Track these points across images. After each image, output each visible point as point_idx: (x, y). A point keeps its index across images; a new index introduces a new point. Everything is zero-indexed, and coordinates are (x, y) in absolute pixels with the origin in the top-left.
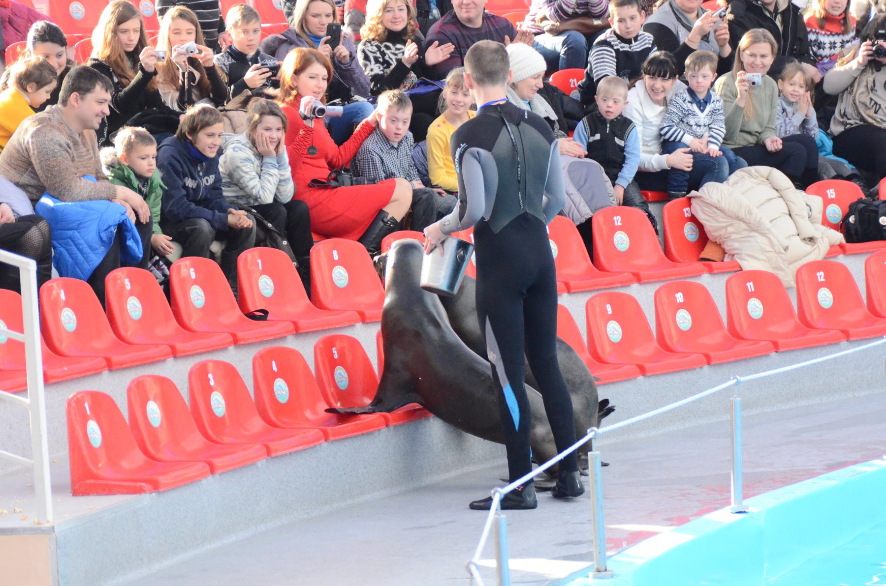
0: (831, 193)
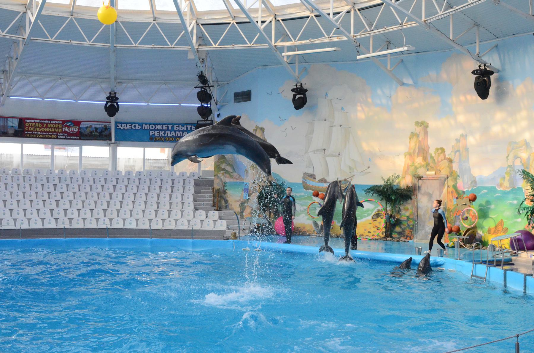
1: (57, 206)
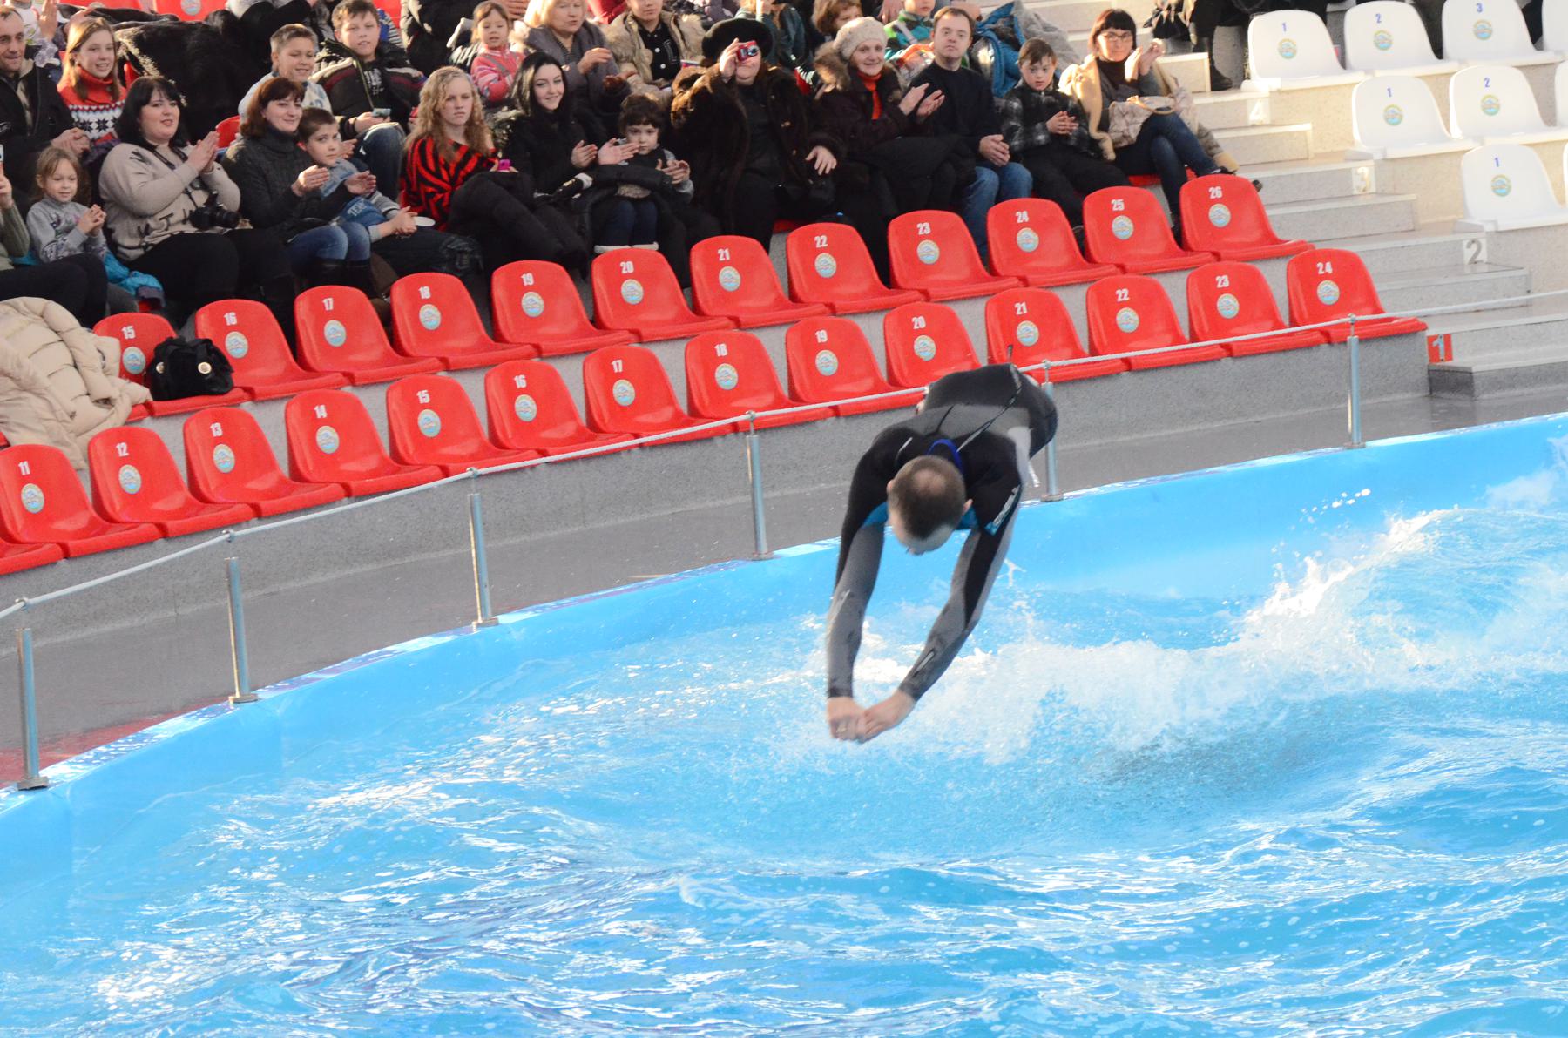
0: (129, 332)
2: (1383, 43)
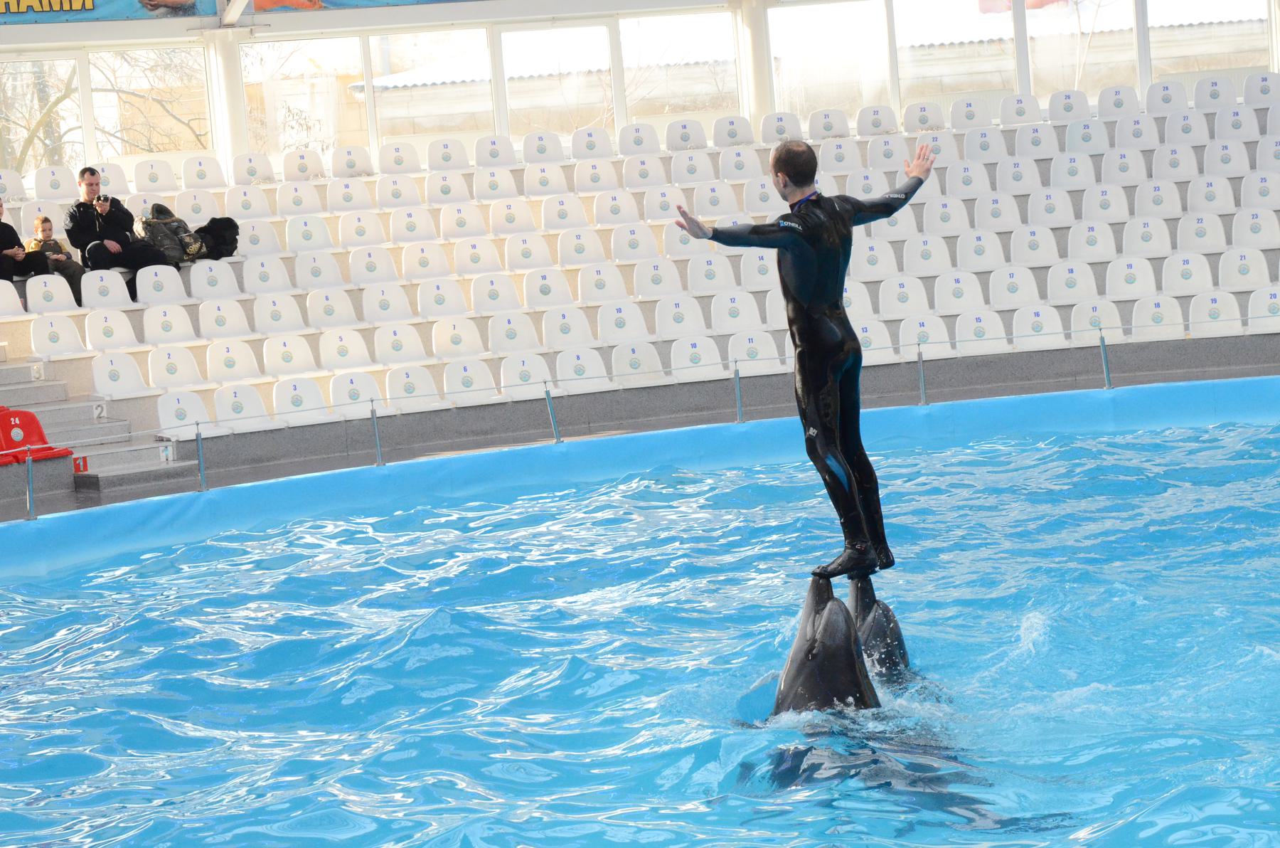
1: (1063, 253)
2: (48, 297)
